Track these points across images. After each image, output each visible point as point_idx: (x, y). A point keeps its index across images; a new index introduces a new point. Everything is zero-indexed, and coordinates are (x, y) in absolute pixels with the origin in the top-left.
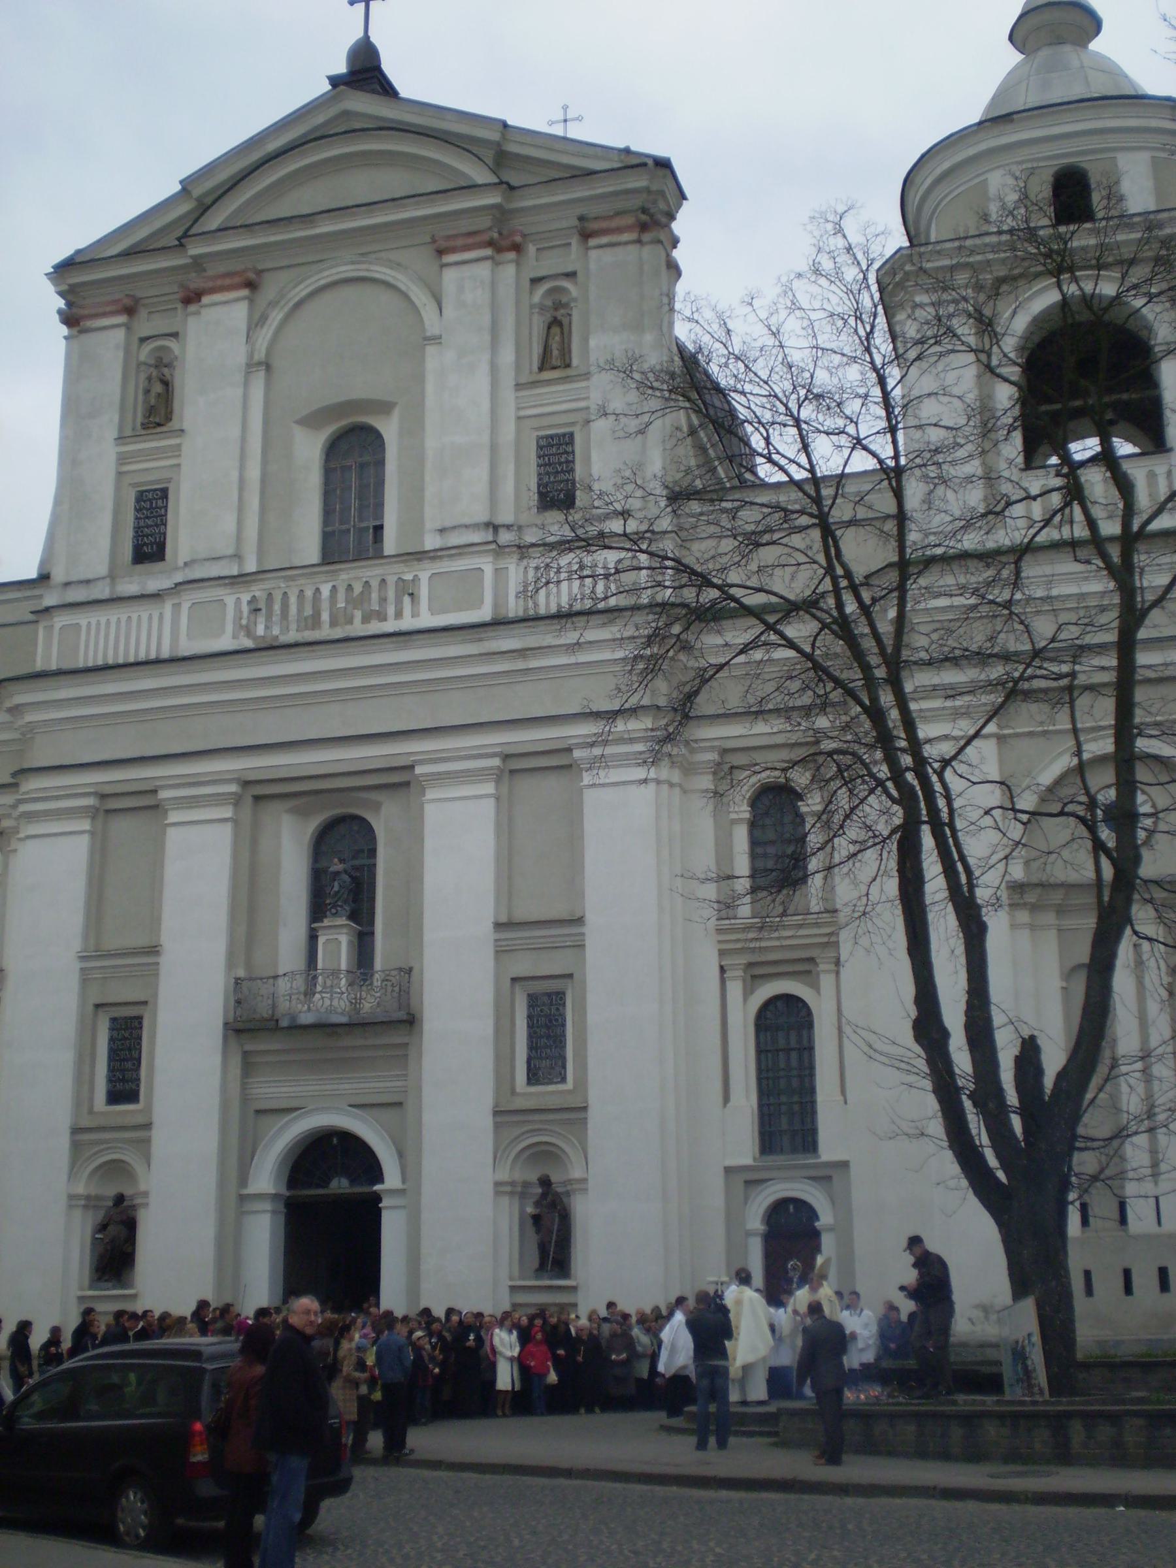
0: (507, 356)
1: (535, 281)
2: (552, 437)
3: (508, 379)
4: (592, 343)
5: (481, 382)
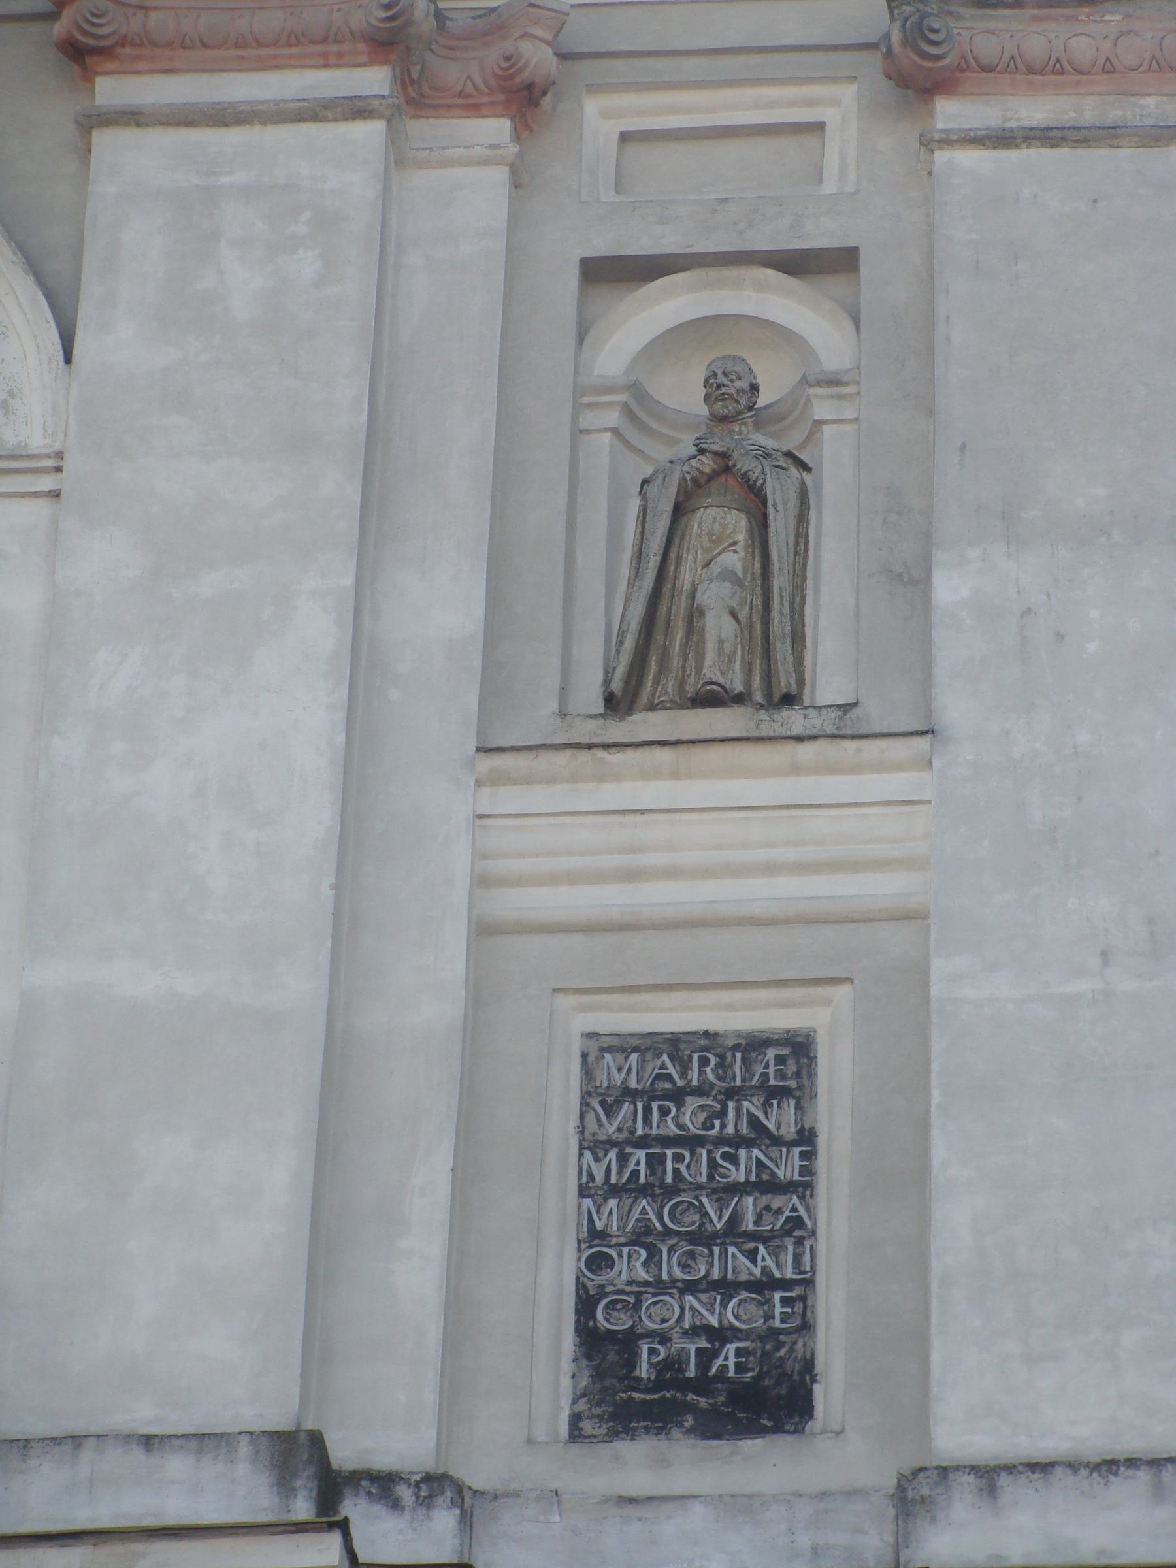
0: (440, 605)
1: (611, 274)
2: (675, 1044)
3: (436, 717)
4: (949, 588)
5: (291, 709)
